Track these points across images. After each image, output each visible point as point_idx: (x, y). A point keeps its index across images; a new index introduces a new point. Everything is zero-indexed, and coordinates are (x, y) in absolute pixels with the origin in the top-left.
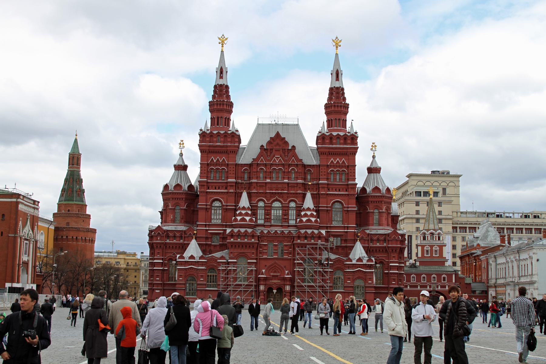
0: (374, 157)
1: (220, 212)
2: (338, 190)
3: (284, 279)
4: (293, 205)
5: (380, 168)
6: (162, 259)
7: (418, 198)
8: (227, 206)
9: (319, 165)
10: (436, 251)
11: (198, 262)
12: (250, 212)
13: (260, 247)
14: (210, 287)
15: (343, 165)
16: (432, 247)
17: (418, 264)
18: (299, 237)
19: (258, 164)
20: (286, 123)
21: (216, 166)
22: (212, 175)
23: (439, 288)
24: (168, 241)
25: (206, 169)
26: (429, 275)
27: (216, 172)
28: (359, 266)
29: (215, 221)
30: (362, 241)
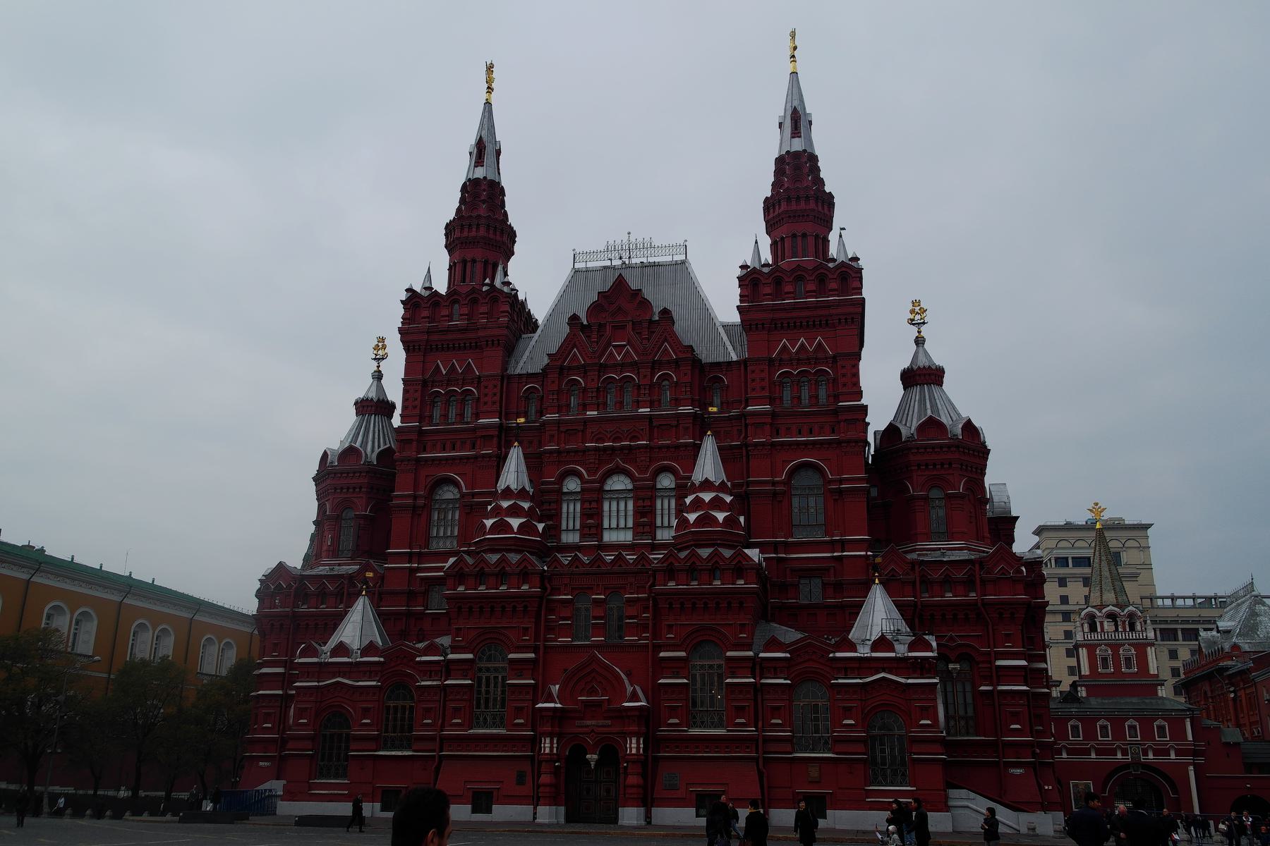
0: (919, 341)
1: (457, 517)
4: (666, 481)
7: (1062, 571)
8: (474, 495)
13: (551, 611)
14: (394, 748)
15: (820, 355)
17: (1082, 692)
18: (670, 572)
19: (562, 368)
20: (651, 260)
21: (448, 385)
22: (437, 413)
23: (1151, 756)
24: (304, 609)
25: (418, 395)
26: (1118, 722)
27: (447, 403)
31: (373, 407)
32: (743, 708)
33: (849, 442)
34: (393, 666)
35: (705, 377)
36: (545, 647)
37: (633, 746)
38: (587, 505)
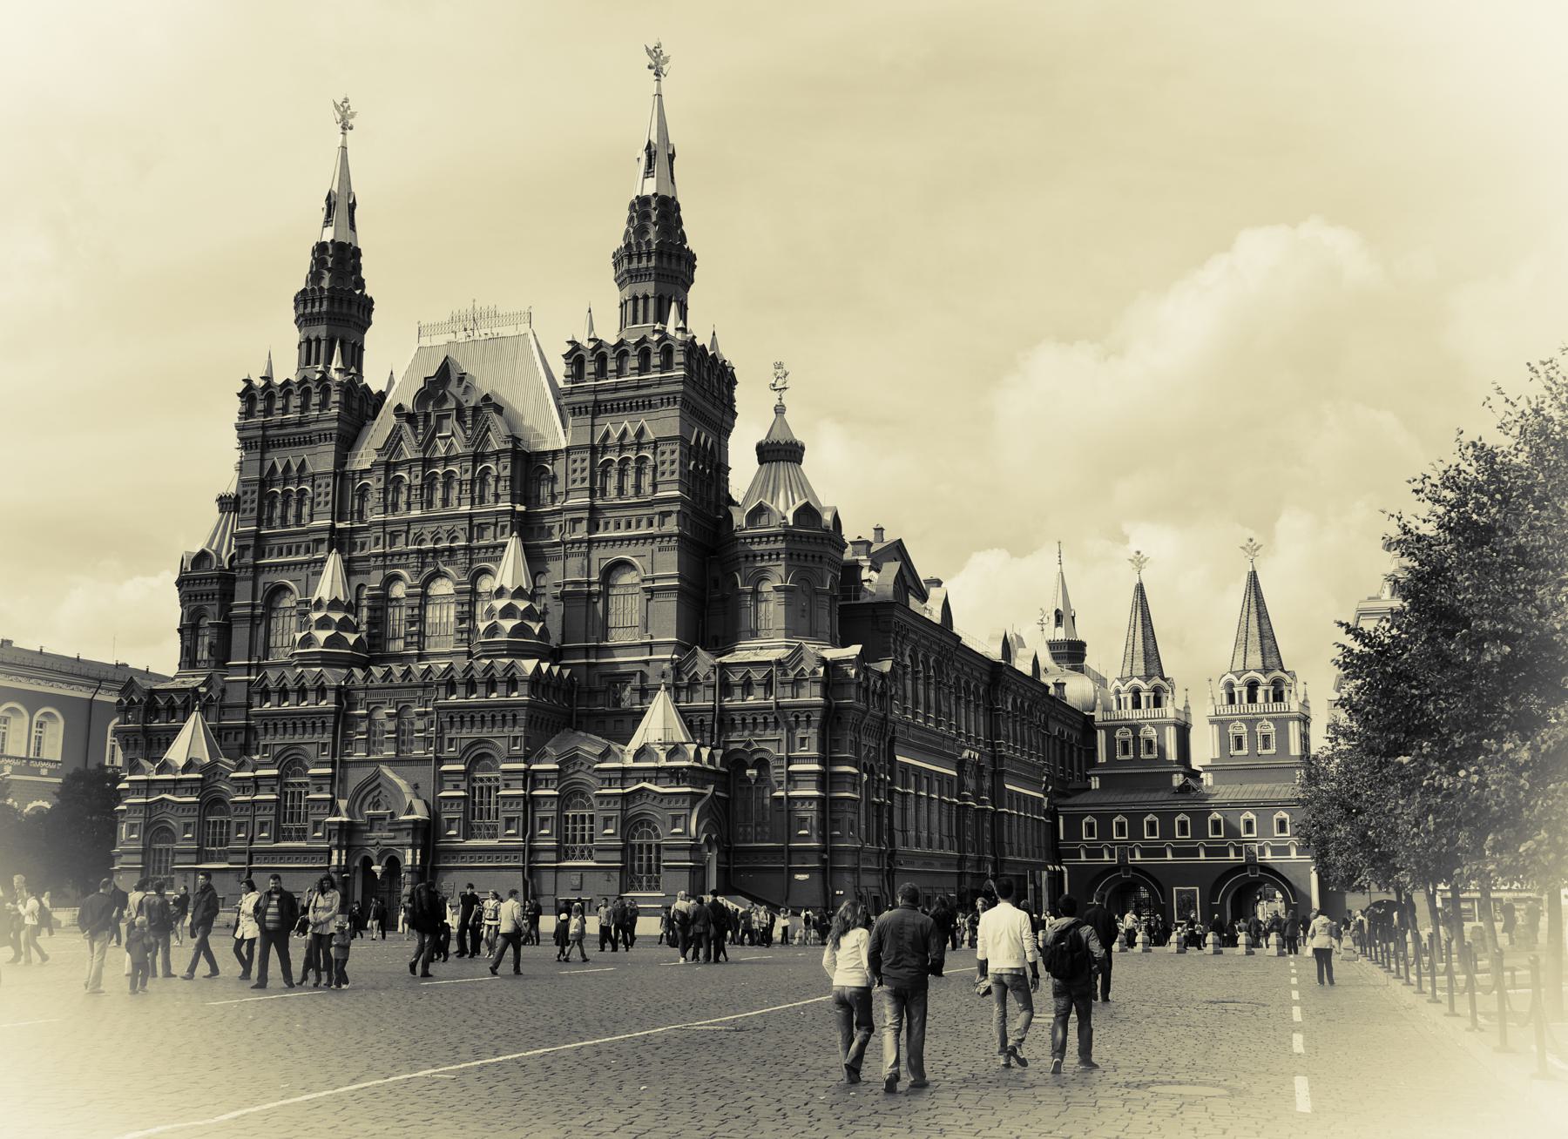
0: (780, 410)
2: (623, 525)
3: (397, 827)
9: (568, 450)
11: (180, 781)
14: (213, 861)
24: (156, 724)
28: (646, 775)
30: (675, 690)
32: (513, 819)
33: (662, 536)
34: (206, 783)
35: (530, 467)
36: (342, 761)
37: (408, 857)
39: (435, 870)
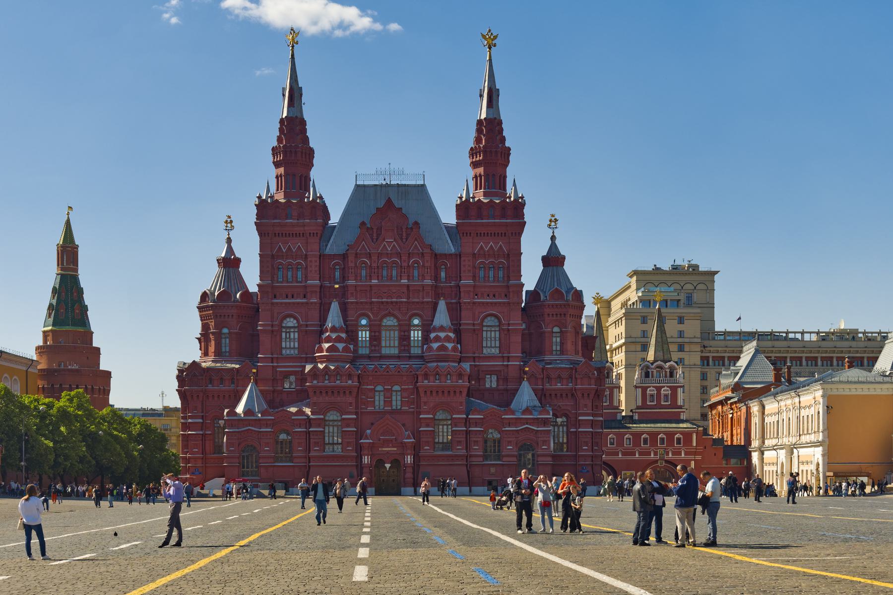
0: (553, 238)
1: (296, 335)
2: (491, 296)
3: (403, 445)
5: (564, 258)
6: (202, 418)
8: (307, 326)
10: (666, 396)
12: (344, 335)
14: (281, 462)
16: (659, 389)
17: (636, 417)
23: (670, 455)
28: (527, 421)
29: (288, 352)
30: (532, 379)
31: (230, 263)
32: (460, 442)
38: (373, 334)
39: (419, 466)
